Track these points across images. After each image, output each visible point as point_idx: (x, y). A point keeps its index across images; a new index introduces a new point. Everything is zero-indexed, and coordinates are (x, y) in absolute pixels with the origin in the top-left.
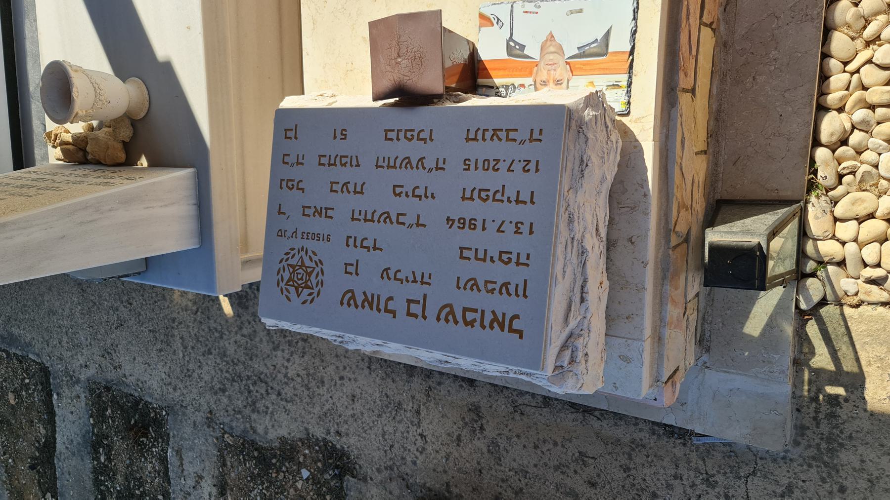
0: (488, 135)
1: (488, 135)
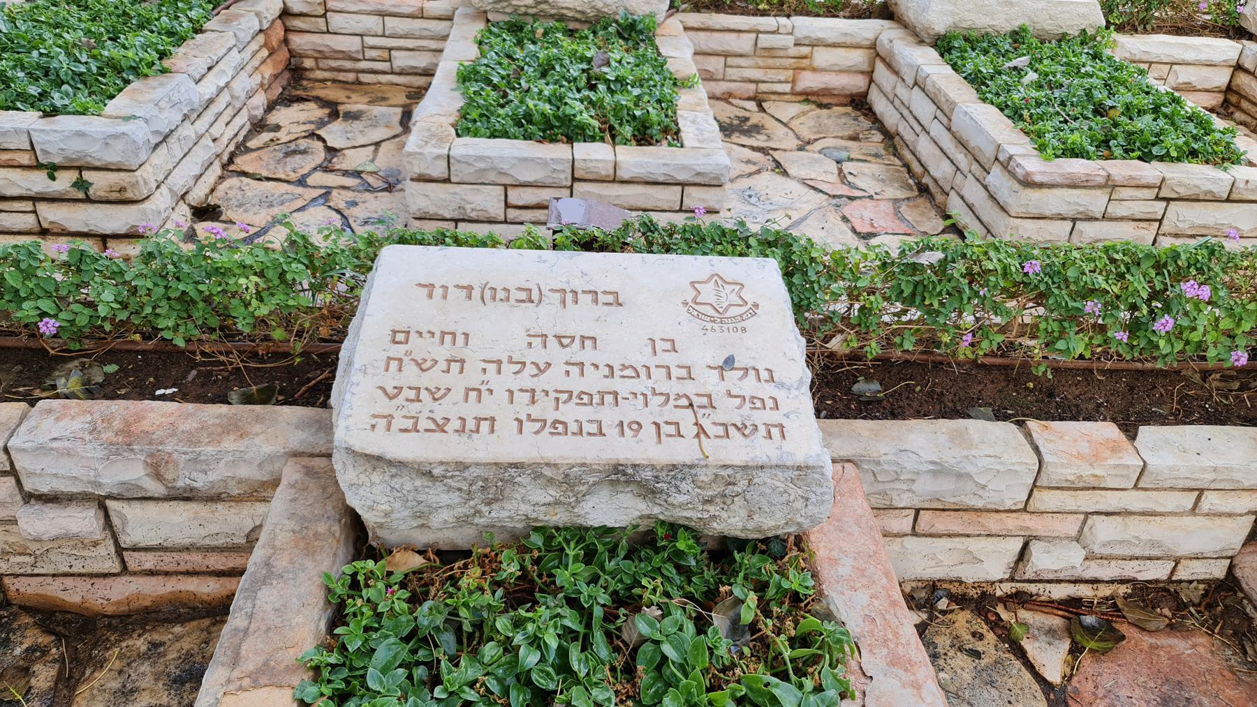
0: (457, 424)
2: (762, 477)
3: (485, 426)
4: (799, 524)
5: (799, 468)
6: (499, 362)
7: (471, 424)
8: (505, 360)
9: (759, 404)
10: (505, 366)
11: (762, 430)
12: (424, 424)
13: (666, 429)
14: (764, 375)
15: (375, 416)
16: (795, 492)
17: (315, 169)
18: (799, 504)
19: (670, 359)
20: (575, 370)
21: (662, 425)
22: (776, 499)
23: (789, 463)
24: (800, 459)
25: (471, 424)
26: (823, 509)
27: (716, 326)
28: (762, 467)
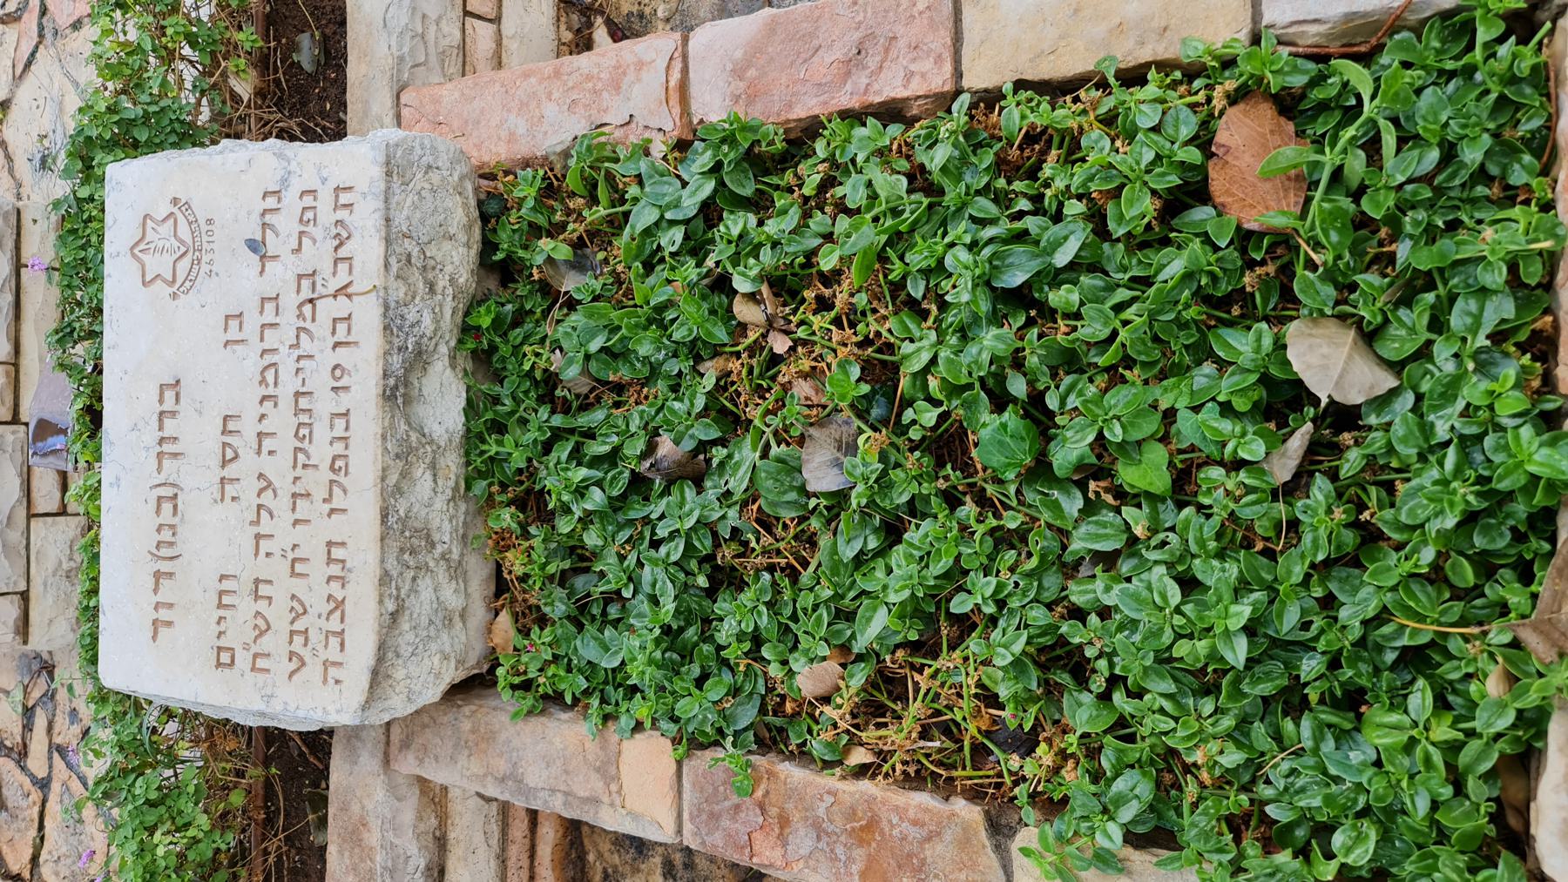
0: (335, 587)
2: (400, 220)
3: (337, 553)
4: (462, 178)
5: (389, 174)
6: (258, 537)
7: (335, 570)
8: (255, 530)
9: (309, 215)
10: (263, 530)
11: (342, 214)
12: (334, 624)
13: (341, 334)
14: (271, 202)
15: (325, 681)
16: (419, 181)
17: (23, 769)
18: (435, 177)
19: (253, 322)
20: (268, 444)
21: (336, 339)
22: (428, 204)
23: (383, 186)
24: (377, 172)
25: (335, 570)
26: (442, 148)
27: (205, 258)
28: (388, 220)
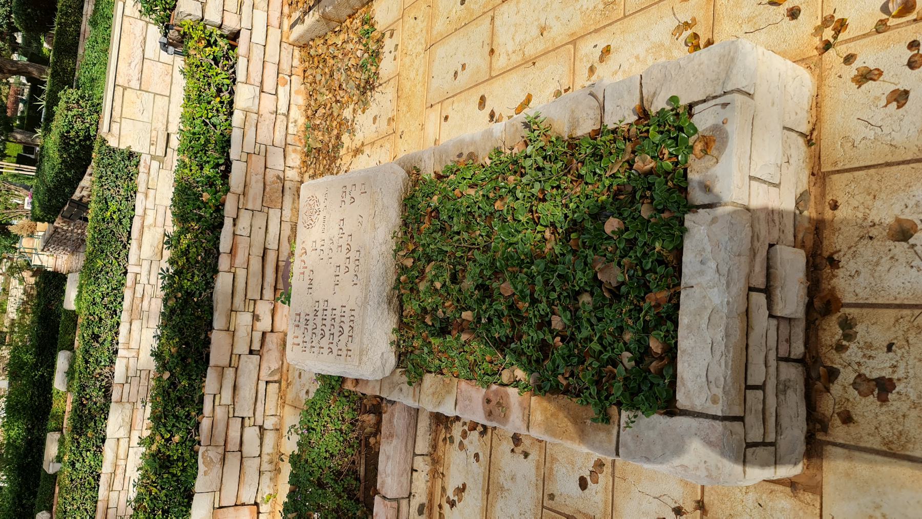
0: (351, 324)
1: (351, 324)
